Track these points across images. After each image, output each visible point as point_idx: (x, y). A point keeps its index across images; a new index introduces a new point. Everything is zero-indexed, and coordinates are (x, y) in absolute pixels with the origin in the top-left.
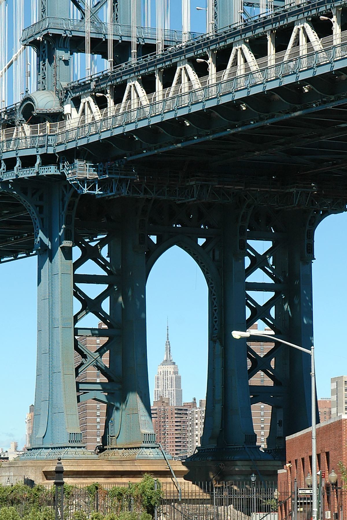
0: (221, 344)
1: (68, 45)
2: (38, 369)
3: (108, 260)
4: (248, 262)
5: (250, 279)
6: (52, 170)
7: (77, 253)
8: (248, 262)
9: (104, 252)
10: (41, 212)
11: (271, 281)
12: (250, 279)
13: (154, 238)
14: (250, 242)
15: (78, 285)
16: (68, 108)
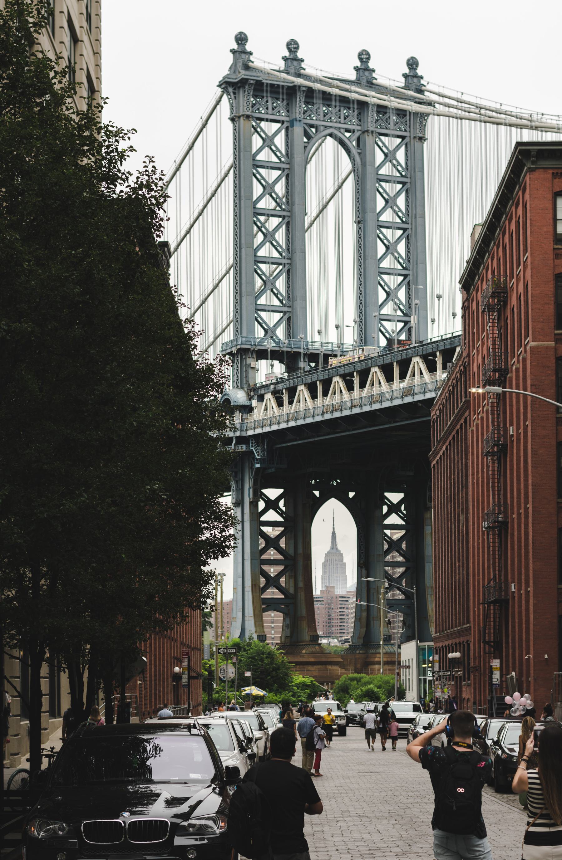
0: (366, 570)
1: (254, 356)
2: (235, 589)
3: (284, 509)
4: (385, 509)
5: (387, 522)
6: (243, 448)
7: (262, 505)
8: (385, 509)
9: (281, 504)
10: (236, 476)
11: (403, 523)
12: (387, 522)
13: (317, 493)
14: (387, 494)
15: (262, 528)
16: (254, 403)
